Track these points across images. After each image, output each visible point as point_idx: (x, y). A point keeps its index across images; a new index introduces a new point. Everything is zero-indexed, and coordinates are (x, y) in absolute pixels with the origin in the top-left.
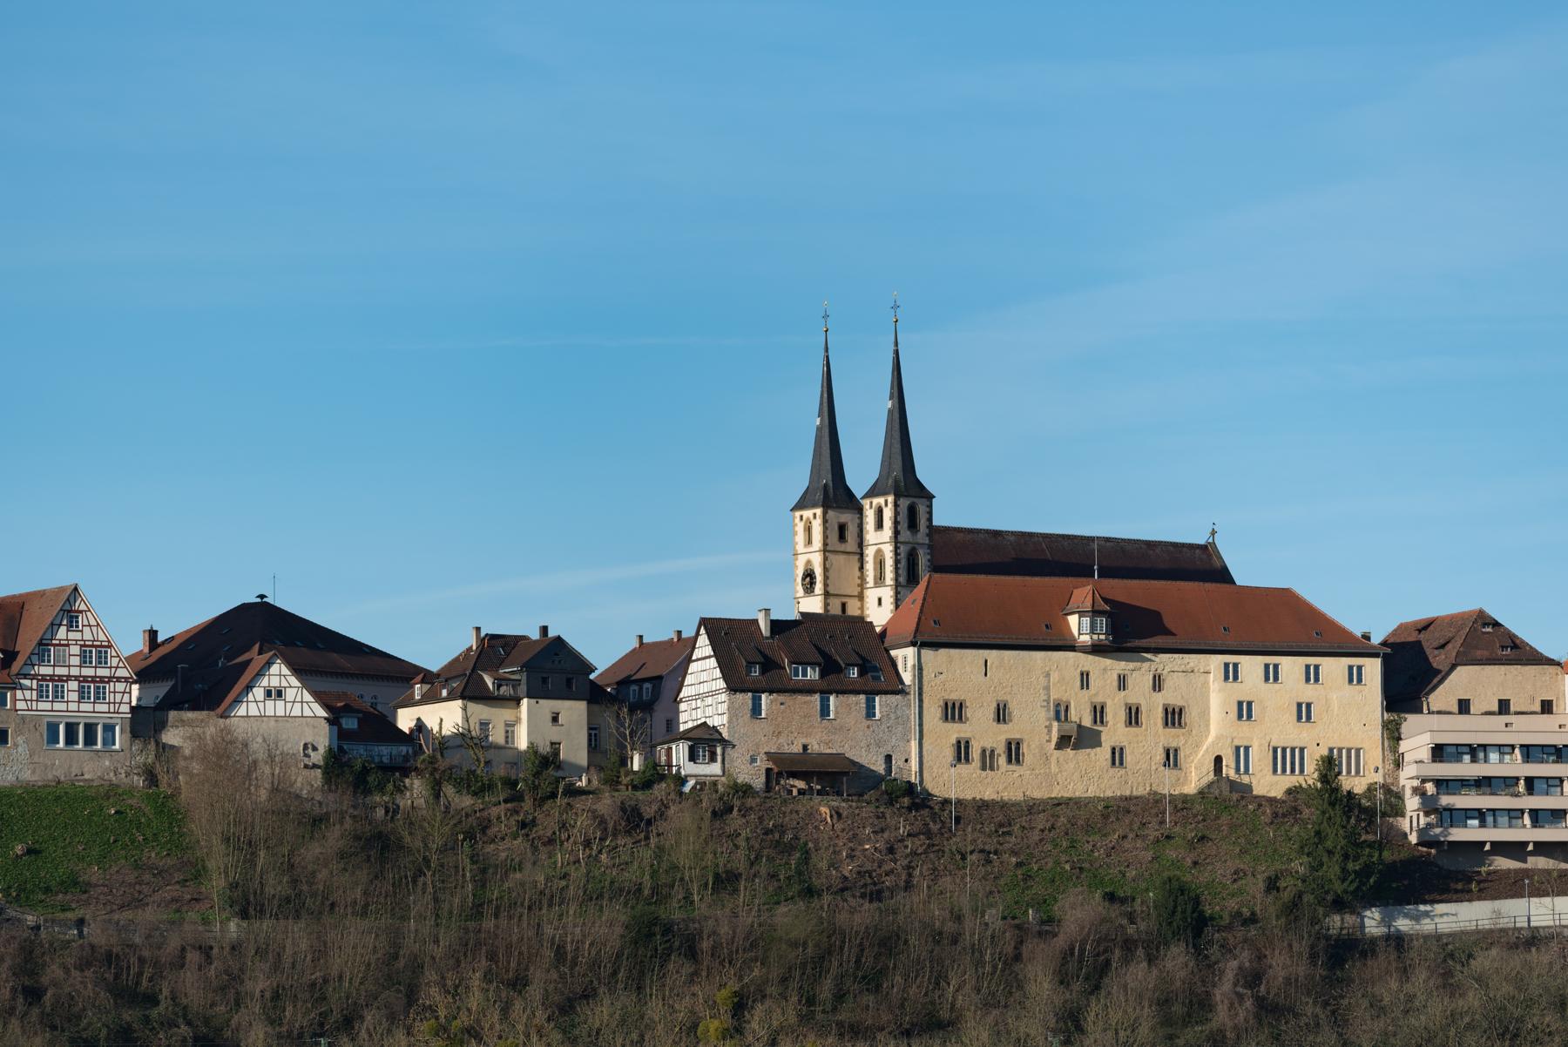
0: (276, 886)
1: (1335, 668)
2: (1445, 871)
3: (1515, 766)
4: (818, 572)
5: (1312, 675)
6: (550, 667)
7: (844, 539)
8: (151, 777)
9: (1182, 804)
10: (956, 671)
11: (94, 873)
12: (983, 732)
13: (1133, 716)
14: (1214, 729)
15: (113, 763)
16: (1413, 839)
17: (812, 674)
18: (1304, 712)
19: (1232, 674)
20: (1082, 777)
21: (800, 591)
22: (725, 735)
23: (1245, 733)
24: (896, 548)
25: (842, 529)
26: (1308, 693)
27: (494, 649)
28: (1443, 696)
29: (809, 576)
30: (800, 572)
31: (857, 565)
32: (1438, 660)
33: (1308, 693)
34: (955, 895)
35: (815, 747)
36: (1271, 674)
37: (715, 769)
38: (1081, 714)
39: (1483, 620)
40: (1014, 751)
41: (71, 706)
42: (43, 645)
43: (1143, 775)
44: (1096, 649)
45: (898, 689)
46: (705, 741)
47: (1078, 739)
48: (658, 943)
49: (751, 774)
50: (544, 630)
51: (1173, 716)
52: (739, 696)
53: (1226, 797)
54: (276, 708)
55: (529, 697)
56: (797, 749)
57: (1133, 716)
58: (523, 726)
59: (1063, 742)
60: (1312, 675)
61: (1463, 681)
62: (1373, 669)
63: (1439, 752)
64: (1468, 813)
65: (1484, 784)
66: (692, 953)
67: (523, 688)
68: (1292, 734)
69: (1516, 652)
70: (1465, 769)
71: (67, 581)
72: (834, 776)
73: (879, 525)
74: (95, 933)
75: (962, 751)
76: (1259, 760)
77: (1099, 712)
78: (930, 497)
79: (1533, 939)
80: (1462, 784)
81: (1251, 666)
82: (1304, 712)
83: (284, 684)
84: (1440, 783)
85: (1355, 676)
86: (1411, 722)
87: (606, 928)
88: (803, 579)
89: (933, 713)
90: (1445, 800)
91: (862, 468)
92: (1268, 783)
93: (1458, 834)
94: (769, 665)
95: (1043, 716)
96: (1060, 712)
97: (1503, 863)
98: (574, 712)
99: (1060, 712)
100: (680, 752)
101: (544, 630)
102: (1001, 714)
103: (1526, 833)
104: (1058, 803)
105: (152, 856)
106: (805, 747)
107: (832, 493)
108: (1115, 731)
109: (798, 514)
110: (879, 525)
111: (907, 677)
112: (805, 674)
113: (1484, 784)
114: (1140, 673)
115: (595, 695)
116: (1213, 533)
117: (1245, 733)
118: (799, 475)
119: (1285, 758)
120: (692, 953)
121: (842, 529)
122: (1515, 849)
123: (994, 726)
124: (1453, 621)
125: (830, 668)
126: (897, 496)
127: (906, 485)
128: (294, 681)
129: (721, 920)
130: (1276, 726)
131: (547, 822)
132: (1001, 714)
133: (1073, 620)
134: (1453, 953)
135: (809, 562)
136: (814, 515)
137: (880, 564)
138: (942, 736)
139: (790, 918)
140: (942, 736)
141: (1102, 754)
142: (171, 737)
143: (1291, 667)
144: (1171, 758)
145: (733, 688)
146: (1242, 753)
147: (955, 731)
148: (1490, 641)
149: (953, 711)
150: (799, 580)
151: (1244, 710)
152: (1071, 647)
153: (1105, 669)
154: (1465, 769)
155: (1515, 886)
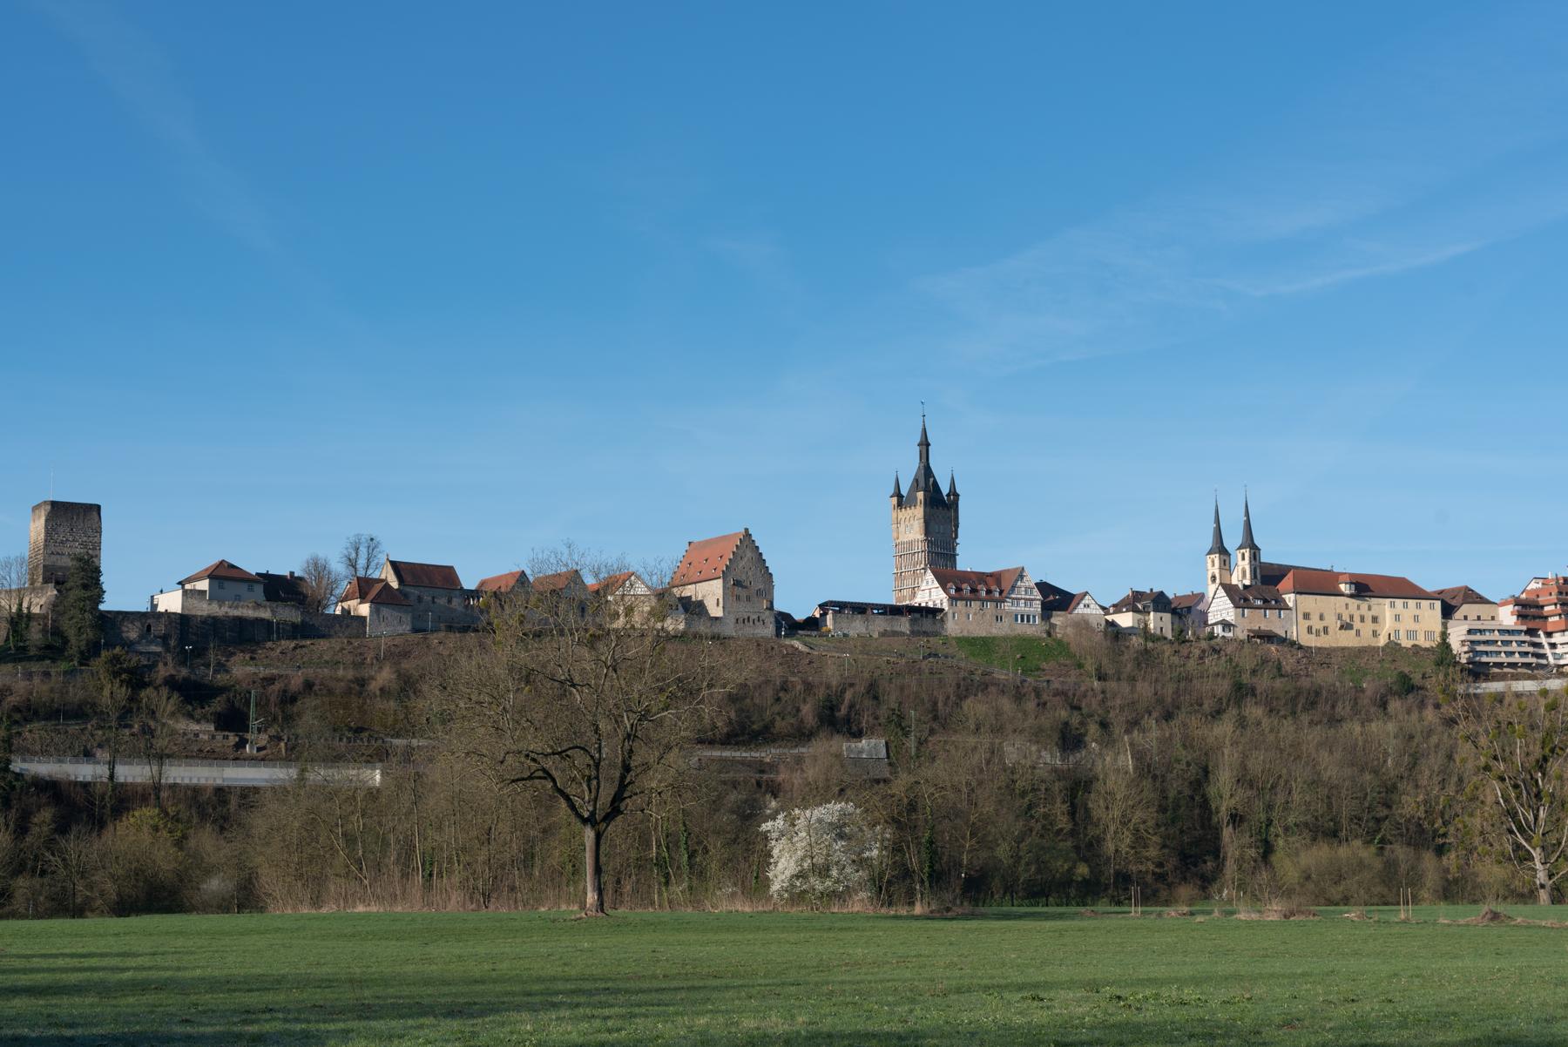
0: (1110, 672)
1: (1425, 603)
2: (1478, 671)
3: (1496, 636)
5: (1418, 606)
6: (1160, 602)
7: (1226, 565)
8: (1049, 634)
9: (1375, 649)
10: (1310, 603)
11: (1044, 665)
12: (1317, 624)
13: (1362, 619)
14: (1388, 625)
15: (1036, 628)
16: (1464, 661)
17: (1259, 603)
18: (1416, 619)
19: (1393, 605)
20: (1347, 640)
23: (1398, 626)
26: (1417, 612)
27: (1138, 595)
28: (1459, 614)
29: (1214, 578)
32: (1453, 603)
33: (1417, 612)
34: (1323, 677)
36: (1405, 606)
37: (1230, 635)
38: (1346, 618)
39: (1467, 589)
40: (1326, 630)
41: (1022, 608)
42: (1013, 587)
43: (1366, 640)
44: (1351, 596)
45: (1289, 609)
46: (1226, 625)
47: (1346, 627)
48: (1241, 692)
49: (1242, 636)
51: (1375, 619)
53: (1393, 647)
54: (1087, 611)
55: (1155, 610)
57: (1362, 619)
58: (1153, 620)
59: (1342, 627)
60: (1418, 606)
61: (1465, 609)
62: (1438, 604)
63: (1470, 632)
64: (1486, 653)
65: (1486, 643)
66: (1254, 695)
68: (1412, 626)
69: (1481, 600)
70: (1478, 637)
71: (1019, 565)
72: (1269, 637)
74: (1056, 685)
75: (1310, 630)
76: (1402, 634)
77: (1351, 617)
79: (1518, 695)
80: (1479, 643)
81: (1399, 602)
82: (1416, 619)
84: (1472, 642)
85: (1432, 607)
86: (1450, 623)
87: (1224, 686)
89: (1300, 616)
90: (1479, 648)
91: (1232, 540)
92: (1406, 643)
93: (1485, 659)
94: (1246, 600)
95: (1334, 618)
96: (1340, 617)
97: (1496, 670)
98: (1167, 617)
99: (1340, 617)
100: (1218, 630)
102: (1321, 617)
103: (1503, 658)
104: (1343, 649)
105: (1062, 660)
107: (1220, 549)
108: (1357, 624)
111: (1291, 605)
113: (1486, 643)
114: (1364, 605)
115: (1174, 612)
117: (1398, 626)
118: (1208, 542)
119: (1411, 634)
120: (1254, 695)
122: (1500, 665)
123: (1308, 621)
124: (1460, 589)
125: (1265, 601)
127: (1250, 543)
129: (1263, 683)
130: (1407, 624)
131: (1185, 651)
132: (1321, 617)
133: (1343, 587)
134: (1499, 698)
136: (1216, 557)
137: (1244, 572)
138: (1305, 624)
139: (1278, 683)
140: (1305, 624)
141: (1353, 632)
142: (1053, 620)
143: (1412, 603)
144: (1375, 634)
145: (1236, 607)
146: (1397, 632)
147: (1307, 623)
148: (1471, 597)
149: (1306, 616)
151: (1397, 618)
152: (1342, 595)
153: (1353, 603)
154: (1478, 637)
155: (1503, 677)
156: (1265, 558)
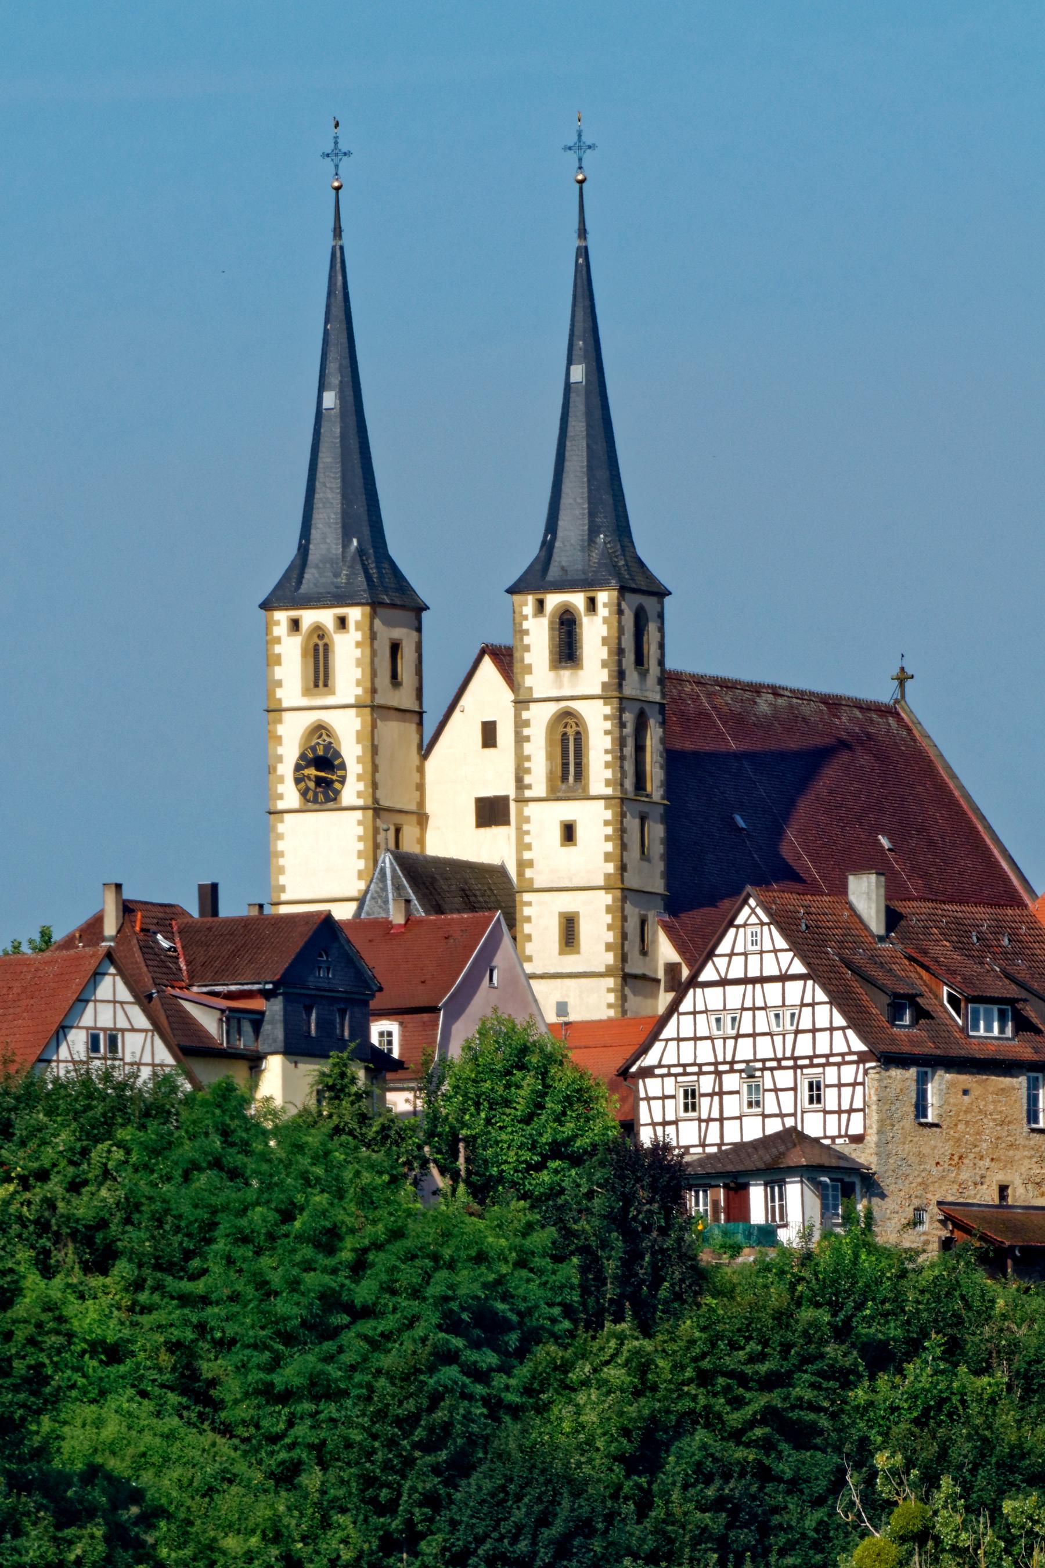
4: (351, 752)
21: (289, 795)
22: (865, 1156)
24: (621, 710)
25: (395, 648)
30: (289, 751)
31: (415, 738)
35: (1020, 1195)
50: (210, 895)
52: (896, 1073)
56: (988, 1195)
67: (274, 1030)
73: (567, 650)
78: (661, 593)
83: (122, 1023)
88: (298, 768)
101: (210, 895)
106: (1003, 1189)
109: (282, 617)
110: (567, 650)
112: (989, 1028)
116: (902, 678)
121: (395, 648)
126: (623, 590)
128: (142, 1021)
135: (320, 729)
150: (286, 769)
156: (691, 648)
